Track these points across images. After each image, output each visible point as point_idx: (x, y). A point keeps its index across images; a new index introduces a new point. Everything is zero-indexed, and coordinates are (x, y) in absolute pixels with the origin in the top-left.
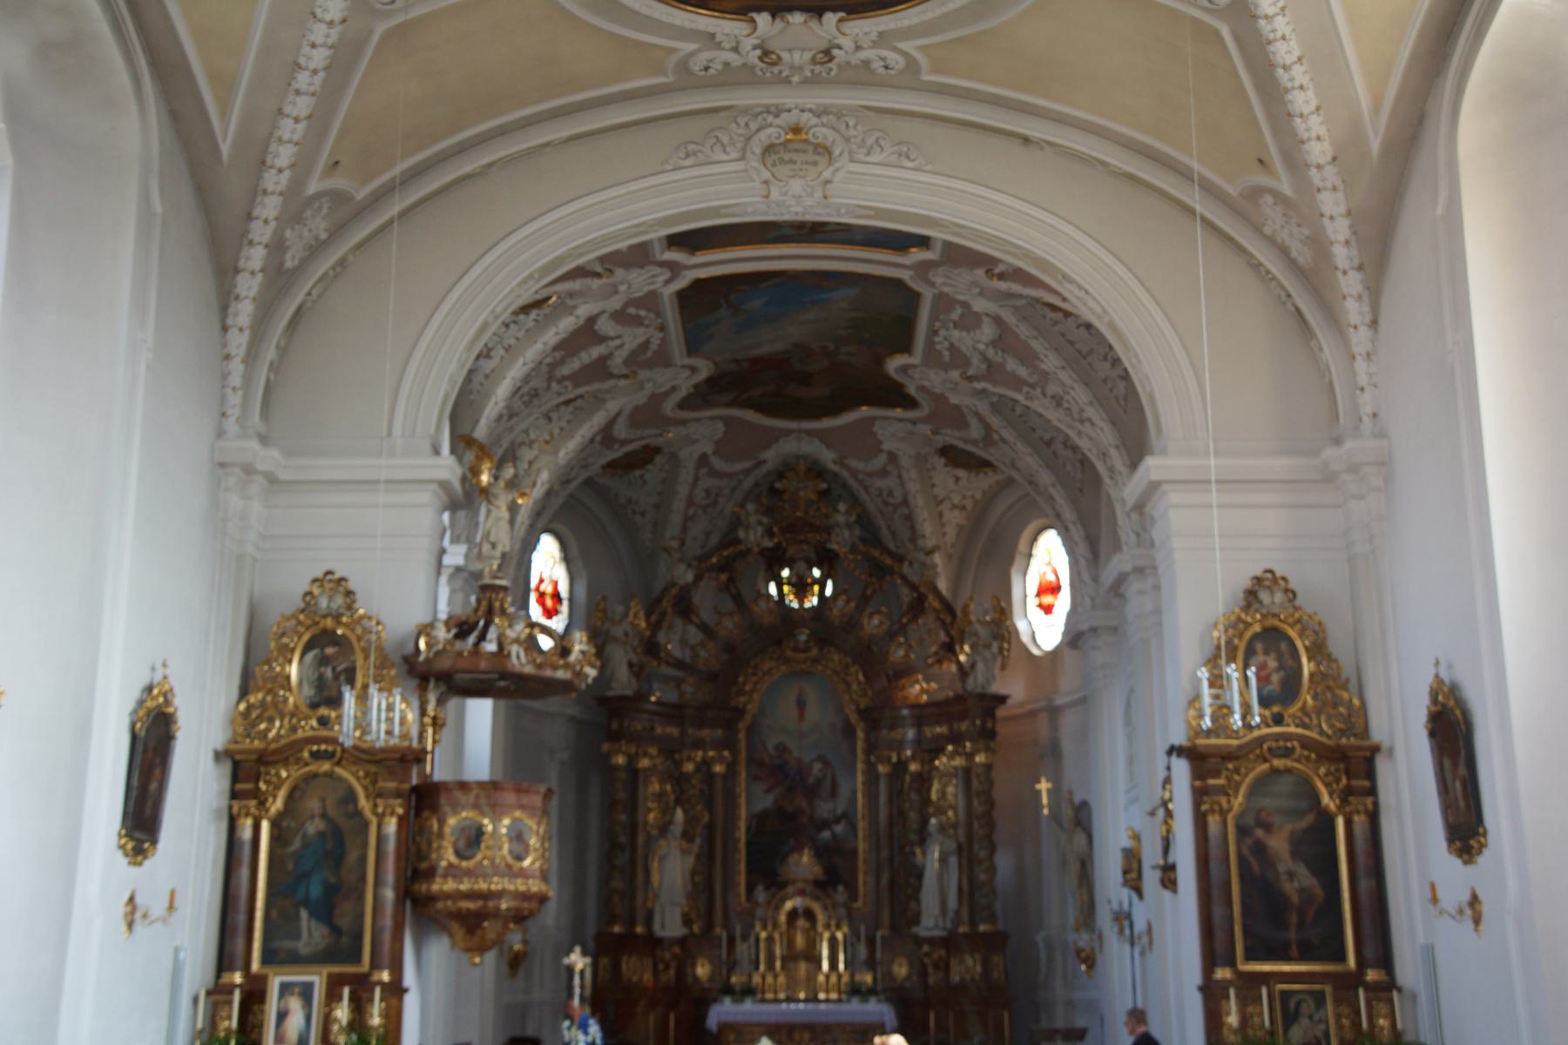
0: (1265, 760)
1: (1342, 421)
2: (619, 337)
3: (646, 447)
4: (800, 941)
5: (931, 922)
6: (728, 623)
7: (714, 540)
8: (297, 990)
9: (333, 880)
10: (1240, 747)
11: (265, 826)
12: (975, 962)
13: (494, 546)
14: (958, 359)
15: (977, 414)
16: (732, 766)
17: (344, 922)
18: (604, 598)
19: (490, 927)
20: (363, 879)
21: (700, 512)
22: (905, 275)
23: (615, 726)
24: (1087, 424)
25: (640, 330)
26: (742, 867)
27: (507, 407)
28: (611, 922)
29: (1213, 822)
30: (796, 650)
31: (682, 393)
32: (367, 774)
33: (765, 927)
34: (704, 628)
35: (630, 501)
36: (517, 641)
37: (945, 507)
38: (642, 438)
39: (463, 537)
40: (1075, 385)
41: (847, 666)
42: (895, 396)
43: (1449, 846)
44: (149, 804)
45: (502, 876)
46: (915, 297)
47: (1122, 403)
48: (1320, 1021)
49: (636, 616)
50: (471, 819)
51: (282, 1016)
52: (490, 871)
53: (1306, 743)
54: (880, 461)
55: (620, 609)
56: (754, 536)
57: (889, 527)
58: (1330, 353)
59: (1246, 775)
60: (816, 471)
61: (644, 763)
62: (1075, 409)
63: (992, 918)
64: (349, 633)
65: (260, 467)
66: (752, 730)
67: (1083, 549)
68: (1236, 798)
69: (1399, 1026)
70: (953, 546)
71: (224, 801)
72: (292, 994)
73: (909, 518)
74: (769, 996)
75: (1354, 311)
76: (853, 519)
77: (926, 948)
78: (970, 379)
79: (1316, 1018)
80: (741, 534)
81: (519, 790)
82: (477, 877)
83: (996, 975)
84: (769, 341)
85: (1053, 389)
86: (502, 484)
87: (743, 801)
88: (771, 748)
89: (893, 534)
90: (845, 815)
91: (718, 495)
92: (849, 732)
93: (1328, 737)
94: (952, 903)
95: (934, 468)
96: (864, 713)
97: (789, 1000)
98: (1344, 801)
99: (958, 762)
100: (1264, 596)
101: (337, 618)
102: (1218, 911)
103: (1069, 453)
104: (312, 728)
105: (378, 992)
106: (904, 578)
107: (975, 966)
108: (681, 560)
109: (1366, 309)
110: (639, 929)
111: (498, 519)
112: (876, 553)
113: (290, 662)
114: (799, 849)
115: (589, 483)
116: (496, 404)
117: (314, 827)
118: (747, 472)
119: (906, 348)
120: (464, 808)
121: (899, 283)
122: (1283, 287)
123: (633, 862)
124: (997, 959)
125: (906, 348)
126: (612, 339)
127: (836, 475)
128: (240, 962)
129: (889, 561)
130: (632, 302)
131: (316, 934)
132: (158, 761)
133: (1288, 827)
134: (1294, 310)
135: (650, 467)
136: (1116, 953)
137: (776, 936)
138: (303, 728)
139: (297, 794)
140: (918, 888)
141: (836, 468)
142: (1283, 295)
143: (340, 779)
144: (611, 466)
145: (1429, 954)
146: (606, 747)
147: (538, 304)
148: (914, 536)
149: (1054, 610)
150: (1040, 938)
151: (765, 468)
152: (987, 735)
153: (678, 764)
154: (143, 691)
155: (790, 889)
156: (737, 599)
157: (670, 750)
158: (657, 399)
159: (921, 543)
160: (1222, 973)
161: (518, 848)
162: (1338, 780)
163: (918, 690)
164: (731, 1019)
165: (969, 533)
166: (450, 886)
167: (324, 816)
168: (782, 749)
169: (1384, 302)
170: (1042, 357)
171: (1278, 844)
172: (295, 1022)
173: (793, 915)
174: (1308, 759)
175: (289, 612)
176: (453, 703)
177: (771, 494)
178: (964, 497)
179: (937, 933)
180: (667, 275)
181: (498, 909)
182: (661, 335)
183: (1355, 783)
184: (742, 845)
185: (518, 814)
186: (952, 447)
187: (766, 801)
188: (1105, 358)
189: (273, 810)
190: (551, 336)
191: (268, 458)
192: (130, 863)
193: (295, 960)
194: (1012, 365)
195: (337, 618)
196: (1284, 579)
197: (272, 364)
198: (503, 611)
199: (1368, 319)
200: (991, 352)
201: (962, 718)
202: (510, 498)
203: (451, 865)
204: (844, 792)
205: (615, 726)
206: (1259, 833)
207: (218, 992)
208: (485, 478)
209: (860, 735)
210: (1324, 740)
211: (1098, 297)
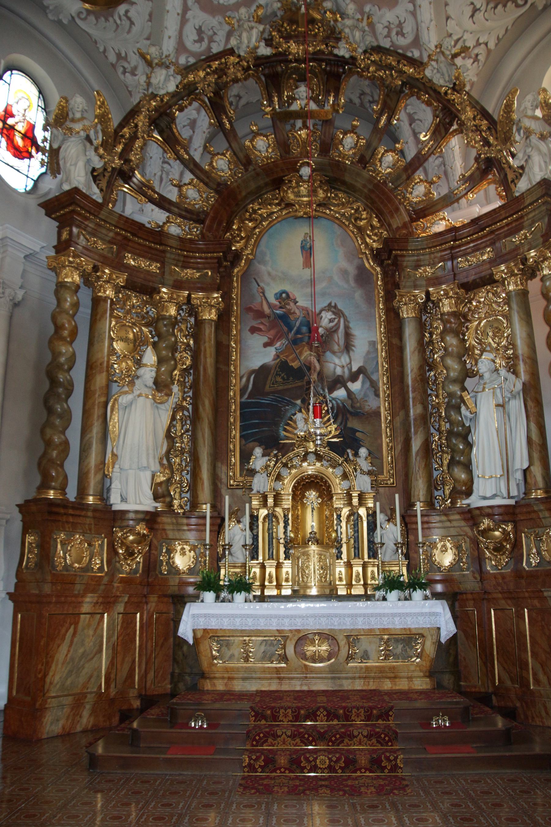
33: (264, 504)
35: (119, 56)
66: (245, 276)
74: (271, 592)
77: (486, 523)
88: (272, 300)
90: (361, 371)
110: (91, 500)
164: (213, 624)
178: (478, 44)
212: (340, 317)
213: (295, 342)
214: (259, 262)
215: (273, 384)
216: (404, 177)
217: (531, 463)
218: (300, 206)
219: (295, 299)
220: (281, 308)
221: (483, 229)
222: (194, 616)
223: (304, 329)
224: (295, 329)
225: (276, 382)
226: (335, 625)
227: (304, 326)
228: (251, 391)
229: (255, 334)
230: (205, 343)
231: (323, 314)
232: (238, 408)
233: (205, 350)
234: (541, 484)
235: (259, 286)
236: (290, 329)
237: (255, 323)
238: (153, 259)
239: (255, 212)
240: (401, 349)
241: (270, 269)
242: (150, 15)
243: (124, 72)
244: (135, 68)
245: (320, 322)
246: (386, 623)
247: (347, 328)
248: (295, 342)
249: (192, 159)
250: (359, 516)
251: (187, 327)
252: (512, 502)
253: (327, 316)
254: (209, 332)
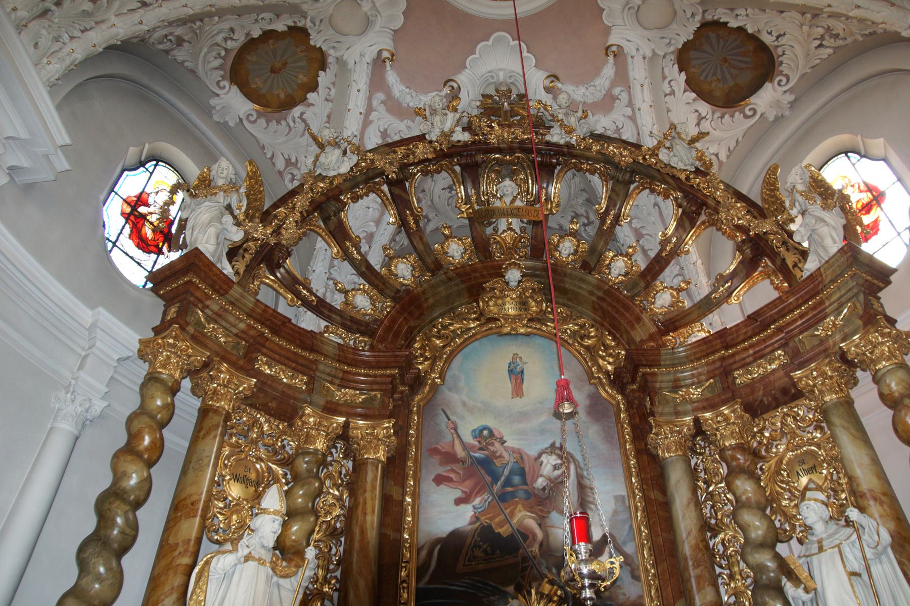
35: (288, 162)
88: (468, 438)
95: (673, 93)
135: (311, 96)
168: (486, 436)
212: (569, 462)
213: (503, 498)
214: (450, 389)
215: (469, 561)
216: (642, 284)
218: (505, 320)
219: (501, 438)
220: (481, 449)
221: (767, 327)
223: (516, 479)
224: (503, 478)
225: (475, 557)
227: (516, 475)
228: (434, 571)
229: (442, 486)
230: (365, 492)
231: (544, 458)
232: (413, 597)
233: (365, 503)
235: (449, 419)
236: (496, 479)
237: (442, 470)
239: (445, 327)
241: (465, 398)
242: (329, 117)
245: (539, 469)
248: (503, 498)
251: (340, 473)
253: (548, 462)
254: (373, 478)
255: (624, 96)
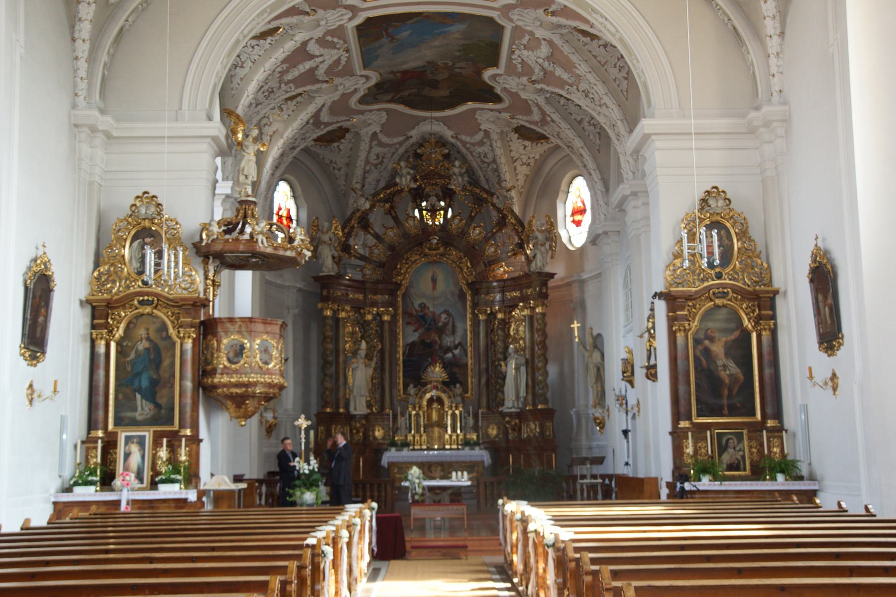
0: (711, 300)
1: (760, 96)
2: (322, 55)
3: (341, 127)
4: (435, 416)
5: (510, 404)
6: (390, 233)
7: (382, 184)
8: (135, 440)
9: (155, 377)
10: (696, 292)
11: (113, 345)
12: (536, 426)
13: (246, 177)
14: (527, 70)
15: (537, 105)
16: (394, 317)
17: (163, 401)
18: (317, 218)
19: (250, 404)
20: (173, 376)
21: (373, 168)
22: (494, 14)
23: (325, 293)
24: (604, 107)
25: (335, 51)
26: (401, 374)
27: (255, 99)
28: (324, 407)
29: (680, 336)
30: (430, 249)
31: (361, 93)
32: (173, 314)
33: (414, 409)
34: (377, 236)
35: (331, 162)
36: (261, 233)
37: (517, 164)
38: (337, 122)
39: (230, 177)
40: (597, 83)
41: (460, 258)
42: (488, 95)
43: (820, 347)
44: (39, 329)
45: (257, 373)
46: (501, 28)
47: (625, 93)
48: (739, 450)
49: (336, 228)
50: (236, 339)
51: (127, 455)
52: (249, 370)
53: (735, 290)
54: (479, 136)
55: (326, 224)
56: (405, 181)
57: (485, 176)
58: (754, 55)
59: (700, 309)
60: (441, 142)
61: (343, 315)
62: (597, 98)
63: (546, 401)
64: (159, 229)
65: (100, 128)
66: (405, 296)
67: (599, 186)
68: (693, 322)
69: (786, 452)
70: (522, 187)
71: (88, 331)
72: (133, 443)
73: (497, 170)
74: (417, 447)
75: (770, 26)
76: (463, 170)
77: (507, 419)
78: (534, 82)
79: (738, 448)
80: (398, 180)
81: (265, 323)
82: (241, 374)
83: (548, 433)
84: (412, 60)
85: (583, 86)
86: (251, 139)
87: (401, 336)
89: (487, 180)
90: (460, 344)
91: (383, 157)
92: (462, 296)
93: (749, 286)
94: (523, 393)
96: (470, 285)
97: (428, 449)
98: (757, 323)
99: (526, 312)
100: (712, 202)
101: (152, 220)
102: (682, 389)
103: (592, 128)
104: (139, 286)
105: (184, 440)
106: (494, 205)
107: (536, 428)
108: (362, 196)
109: (778, 25)
111: (249, 161)
112: (478, 191)
113: (124, 247)
114: (433, 363)
115: (306, 150)
116: (248, 96)
117: (142, 346)
118: (401, 144)
119: (495, 63)
120: (232, 334)
121: (490, 20)
122: (725, 13)
123: (337, 372)
124: (548, 424)
125: (495, 63)
126: (317, 57)
127: (453, 145)
128: (101, 425)
129: (485, 196)
130: (328, 33)
131: (146, 408)
132: (43, 304)
133: (724, 339)
134: (732, 28)
135: (343, 141)
136: (618, 420)
137: (421, 413)
138: (133, 286)
139: (132, 325)
140: (503, 385)
141: (453, 141)
142: (726, 19)
143: (157, 317)
144: (318, 140)
145: (805, 408)
146: (320, 306)
147: (272, 32)
148: (500, 181)
149: (582, 224)
150: (572, 412)
151: (411, 141)
152: (543, 296)
153: (363, 316)
154: (31, 261)
155: (429, 386)
156: (396, 219)
157: (358, 308)
158: (346, 97)
159: (504, 184)
160: (683, 424)
161: (266, 357)
162: (753, 311)
163: (502, 271)
164: (395, 460)
165: (532, 179)
166: (225, 379)
167: (148, 339)
168: (423, 306)
169: (788, 20)
170: (578, 66)
171: (718, 349)
172: (135, 459)
173: (431, 401)
174: (736, 299)
175: (122, 217)
176: (225, 273)
177: (416, 156)
178: (529, 158)
179: (513, 410)
180: (350, 14)
181: (255, 393)
182: (347, 55)
183: (763, 312)
184: (401, 362)
185: (265, 337)
186: (522, 126)
187: (414, 337)
188: (615, 66)
189: (117, 336)
190: (280, 54)
191: (106, 122)
192: (28, 365)
193: (134, 423)
194: (559, 72)
195: (152, 220)
196: (723, 192)
197: (105, 64)
198: (253, 216)
199: (778, 32)
200: (546, 64)
201: (528, 287)
202: (256, 148)
203: (225, 367)
204: (459, 332)
205: (325, 293)
206: (707, 342)
207: (89, 442)
208: (240, 136)
209: (469, 298)
210: (746, 287)
211: (613, 22)
213: (428, 330)
217: (527, 393)
222: (388, 457)
223: (433, 323)
226: (443, 459)
234: (531, 403)
238: (360, 293)
240: (479, 334)
242: (351, 148)
243: (334, 168)
244: (341, 168)
246: (463, 459)
247: (453, 322)
248: (428, 330)
249: (375, 232)
250: (456, 414)
252: (518, 410)
253: (444, 316)
255: (489, 143)
